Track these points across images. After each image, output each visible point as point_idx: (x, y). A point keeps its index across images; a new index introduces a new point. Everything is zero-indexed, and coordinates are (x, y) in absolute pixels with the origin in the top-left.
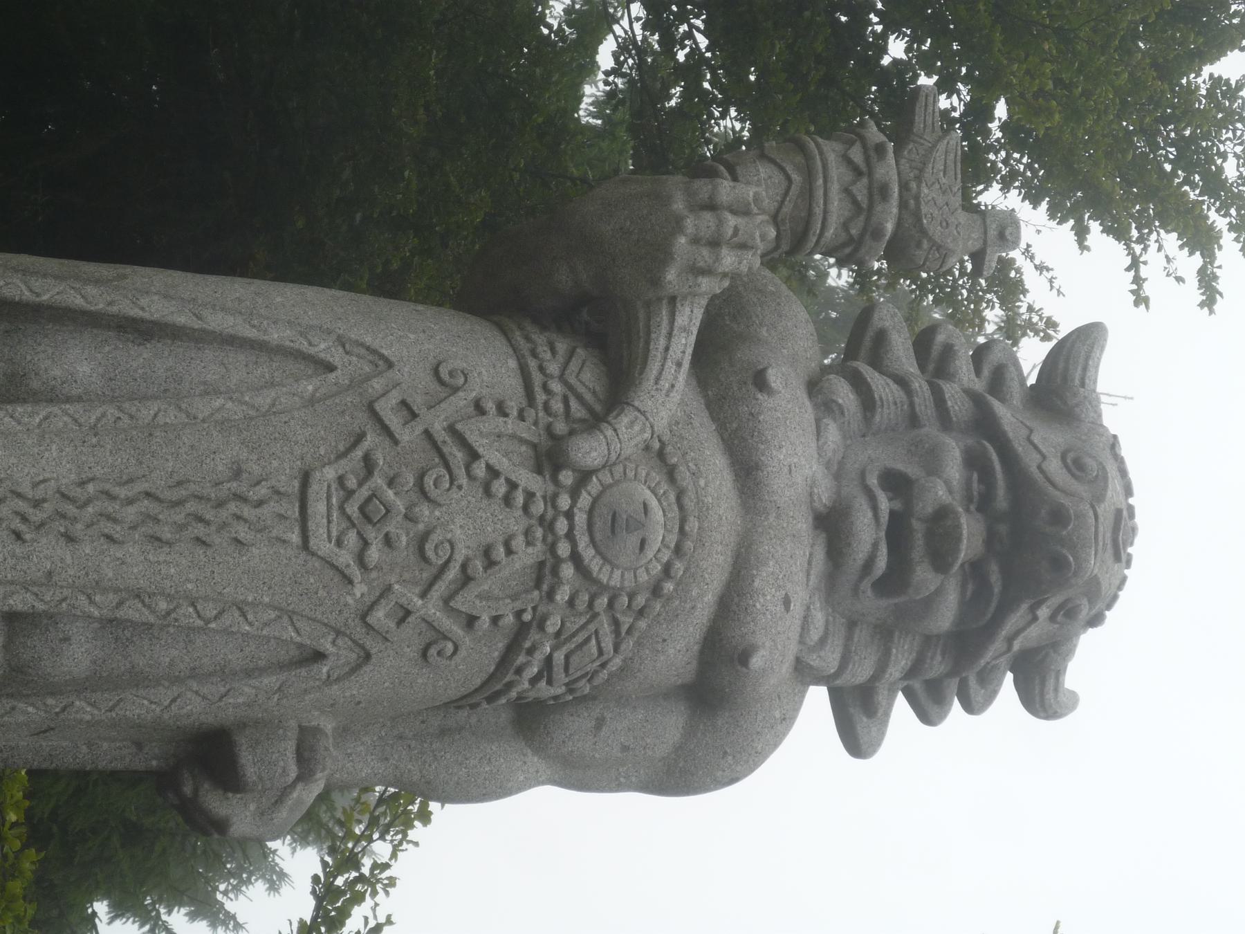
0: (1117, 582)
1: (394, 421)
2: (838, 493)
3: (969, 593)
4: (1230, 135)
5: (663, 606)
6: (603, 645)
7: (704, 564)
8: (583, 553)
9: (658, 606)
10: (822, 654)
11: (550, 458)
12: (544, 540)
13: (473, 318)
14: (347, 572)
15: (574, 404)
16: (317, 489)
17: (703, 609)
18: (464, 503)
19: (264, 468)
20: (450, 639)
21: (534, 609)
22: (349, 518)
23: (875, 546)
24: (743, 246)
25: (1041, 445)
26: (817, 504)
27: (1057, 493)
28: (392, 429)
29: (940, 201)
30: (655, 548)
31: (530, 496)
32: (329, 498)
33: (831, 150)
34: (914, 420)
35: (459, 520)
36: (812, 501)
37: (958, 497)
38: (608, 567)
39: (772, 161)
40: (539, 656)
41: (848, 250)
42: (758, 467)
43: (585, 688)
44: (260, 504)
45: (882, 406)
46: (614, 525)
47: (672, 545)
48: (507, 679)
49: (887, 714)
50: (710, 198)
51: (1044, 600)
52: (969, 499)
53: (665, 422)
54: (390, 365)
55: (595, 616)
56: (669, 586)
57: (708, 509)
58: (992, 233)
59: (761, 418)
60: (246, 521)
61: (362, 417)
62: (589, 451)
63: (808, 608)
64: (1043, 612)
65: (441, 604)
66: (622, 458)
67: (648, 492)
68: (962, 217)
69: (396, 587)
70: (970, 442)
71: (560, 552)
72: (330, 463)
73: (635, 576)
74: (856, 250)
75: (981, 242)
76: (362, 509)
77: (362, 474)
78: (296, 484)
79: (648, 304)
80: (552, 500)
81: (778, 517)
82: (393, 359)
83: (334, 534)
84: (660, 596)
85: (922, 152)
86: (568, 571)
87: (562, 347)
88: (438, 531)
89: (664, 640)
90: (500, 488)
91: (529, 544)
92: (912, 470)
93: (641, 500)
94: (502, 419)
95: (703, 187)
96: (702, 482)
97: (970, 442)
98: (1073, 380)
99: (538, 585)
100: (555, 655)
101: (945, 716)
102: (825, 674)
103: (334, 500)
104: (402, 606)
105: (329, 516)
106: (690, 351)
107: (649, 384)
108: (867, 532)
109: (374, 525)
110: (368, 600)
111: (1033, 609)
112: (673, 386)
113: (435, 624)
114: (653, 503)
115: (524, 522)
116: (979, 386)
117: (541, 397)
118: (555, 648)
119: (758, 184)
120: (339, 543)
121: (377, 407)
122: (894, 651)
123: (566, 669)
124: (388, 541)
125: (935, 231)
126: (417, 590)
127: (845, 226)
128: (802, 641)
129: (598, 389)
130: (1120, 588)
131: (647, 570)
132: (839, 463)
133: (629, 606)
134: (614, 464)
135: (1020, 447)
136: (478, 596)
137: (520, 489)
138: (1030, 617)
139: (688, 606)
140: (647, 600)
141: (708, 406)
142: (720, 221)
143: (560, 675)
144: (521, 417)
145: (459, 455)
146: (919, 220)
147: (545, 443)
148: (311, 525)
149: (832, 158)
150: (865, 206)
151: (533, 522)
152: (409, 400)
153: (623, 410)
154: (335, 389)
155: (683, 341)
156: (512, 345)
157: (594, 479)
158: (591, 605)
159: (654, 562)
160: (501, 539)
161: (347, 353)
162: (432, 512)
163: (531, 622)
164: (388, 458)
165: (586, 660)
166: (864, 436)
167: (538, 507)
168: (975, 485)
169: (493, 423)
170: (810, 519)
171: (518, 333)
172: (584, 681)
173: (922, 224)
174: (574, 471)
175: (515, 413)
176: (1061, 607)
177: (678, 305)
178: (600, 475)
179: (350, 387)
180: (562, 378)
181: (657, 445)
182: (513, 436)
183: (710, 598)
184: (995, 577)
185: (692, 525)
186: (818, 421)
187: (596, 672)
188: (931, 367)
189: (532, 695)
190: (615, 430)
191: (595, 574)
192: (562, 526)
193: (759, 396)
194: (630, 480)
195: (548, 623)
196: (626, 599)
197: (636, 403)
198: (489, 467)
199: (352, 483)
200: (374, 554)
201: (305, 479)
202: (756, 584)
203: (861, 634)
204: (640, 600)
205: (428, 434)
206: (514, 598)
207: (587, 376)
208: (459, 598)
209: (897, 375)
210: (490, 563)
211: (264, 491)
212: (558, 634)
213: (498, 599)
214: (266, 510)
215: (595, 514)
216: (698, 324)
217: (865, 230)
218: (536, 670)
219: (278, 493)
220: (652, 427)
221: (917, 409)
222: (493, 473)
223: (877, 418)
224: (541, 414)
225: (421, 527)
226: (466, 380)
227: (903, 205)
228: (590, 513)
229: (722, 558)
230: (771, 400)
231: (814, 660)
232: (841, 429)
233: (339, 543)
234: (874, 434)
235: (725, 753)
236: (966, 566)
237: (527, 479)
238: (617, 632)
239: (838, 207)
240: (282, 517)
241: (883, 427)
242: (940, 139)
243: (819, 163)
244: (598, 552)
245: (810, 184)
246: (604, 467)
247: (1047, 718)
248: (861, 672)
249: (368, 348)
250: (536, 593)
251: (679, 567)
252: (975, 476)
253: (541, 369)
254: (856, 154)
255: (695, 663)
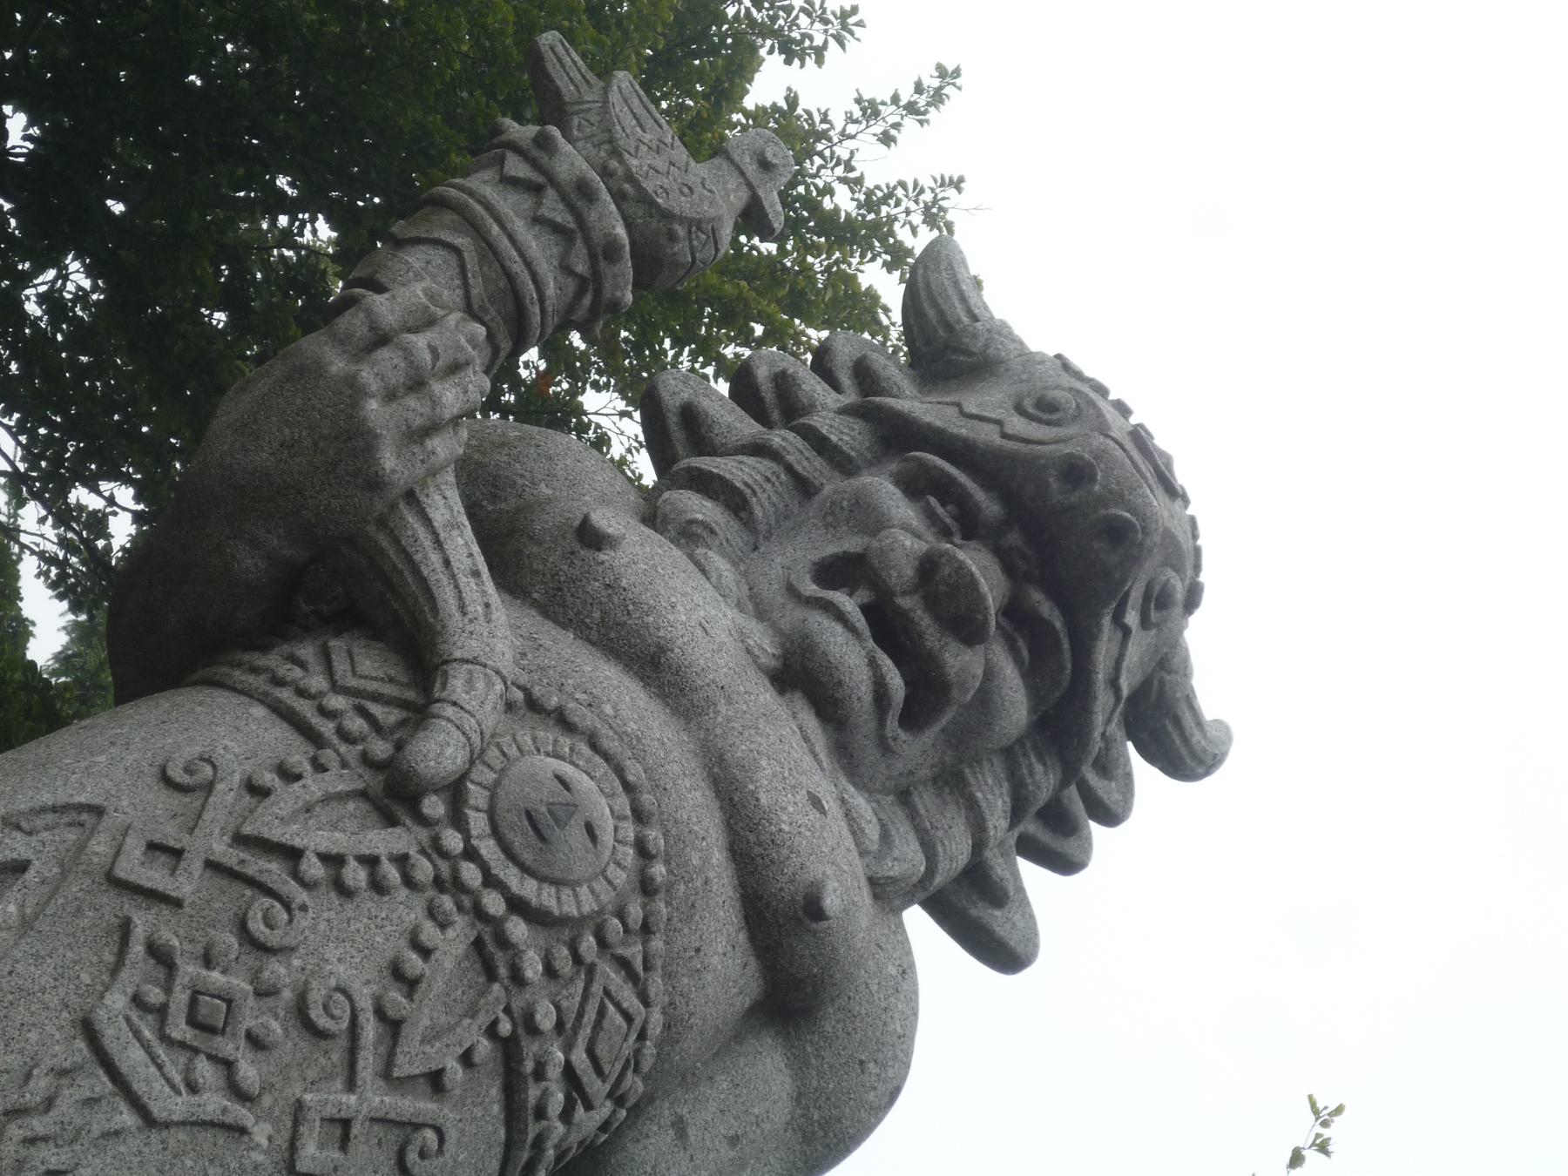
0: (1188, 528)
1: (155, 877)
2: (778, 631)
3: (1025, 653)
4: (818, 161)
5: (668, 904)
6: (625, 1005)
7: (683, 815)
8: (523, 893)
9: (660, 905)
10: (896, 853)
11: (395, 794)
12: (460, 909)
13: (167, 694)
14: (229, 1119)
15: (376, 709)
16: (114, 1034)
17: (719, 877)
18: (322, 926)
19: (21, 1052)
20: (424, 1125)
21: (508, 1010)
22: (183, 1045)
23: (872, 663)
24: (455, 368)
25: (981, 413)
26: (763, 660)
27: (1052, 447)
28: (161, 889)
29: (660, 163)
30: (610, 828)
31: (402, 860)
32: (137, 1034)
33: (483, 183)
34: (804, 488)
35: (332, 953)
36: (755, 659)
37: (931, 538)
38: (567, 891)
39: (418, 241)
40: (554, 1072)
41: (587, 300)
42: (662, 649)
43: (635, 1085)
44: (49, 1103)
45: (754, 492)
46: (539, 828)
47: (629, 812)
48: (531, 1136)
49: (1020, 889)
50: (372, 329)
51: (1127, 594)
52: (946, 533)
53: (509, 656)
54: (98, 811)
55: (591, 970)
56: (659, 870)
57: (639, 740)
58: (751, 169)
59: (624, 583)
60: (45, 1139)
61: (112, 905)
62: (439, 751)
63: (843, 801)
64: (1132, 618)
65: (382, 1084)
66: (487, 736)
67: (549, 760)
68: (700, 170)
69: (308, 1097)
70: (894, 467)
71: (492, 911)
72: (107, 988)
73: (610, 882)
74: (598, 293)
75: (745, 189)
76: (192, 1021)
77: (161, 974)
78: (81, 1044)
79: (382, 522)
80: (436, 848)
81: (729, 702)
82: (97, 801)
83: (178, 1079)
84: (656, 892)
85: (594, 118)
86: (518, 929)
87: (307, 651)
88: (314, 984)
89: (698, 950)
90: (356, 875)
91: (443, 926)
92: (852, 544)
93: (550, 775)
94: (296, 786)
95: (352, 322)
96: (608, 710)
97: (894, 467)
98: (959, 321)
99: (491, 974)
100: (573, 1058)
101: (1090, 845)
102: (915, 879)
103: (147, 1034)
104: (332, 1120)
105: (154, 1059)
106: (476, 549)
107: (455, 621)
108: (851, 655)
109: (223, 1032)
110: (282, 1141)
111: (1118, 619)
112: (487, 605)
113: (392, 1116)
114: (568, 770)
115: (418, 903)
116: (850, 397)
117: (327, 728)
118: (568, 1048)
119: (418, 277)
120: (193, 1088)
121: (120, 873)
122: (979, 795)
123: (599, 1071)
124: (256, 1042)
125: (681, 205)
126: (339, 1084)
127: (565, 268)
128: (863, 853)
129: (393, 672)
130: (1195, 537)
131: (618, 864)
132: (750, 598)
133: (627, 930)
134: (483, 751)
135: (962, 429)
136: (425, 1040)
137: (384, 859)
138: (1119, 634)
139: (698, 883)
140: (644, 906)
141: (545, 613)
142: (405, 349)
143: (597, 1088)
144: (319, 767)
145: (274, 866)
146: (653, 203)
147: (375, 782)
148: (138, 1087)
149: (490, 192)
150: (572, 225)
151: (430, 893)
152: (157, 838)
153: (446, 673)
154: (46, 889)
155: (461, 541)
156: (241, 692)
157: (469, 785)
158: (577, 959)
159: (620, 848)
160: (403, 943)
161: (30, 834)
162: (289, 966)
163: (514, 1031)
164: (181, 932)
165: (616, 1044)
166: (756, 548)
167: (424, 870)
168: (940, 510)
169: (287, 798)
170: (767, 682)
171: (237, 673)
172: (630, 1073)
173: (658, 206)
174: (436, 792)
175: (307, 767)
176: (1147, 597)
177: (422, 498)
178: (474, 776)
179: (64, 873)
180: (336, 688)
181: (519, 695)
182: (327, 799)
183: (718, 857)
184: (1046, 608)
185: (634, 772)
186: (691, 556)
187: (637, 1052)
188: (775, 415)
189: (574, 1139)
190: (455, 704)
191: (556, 912)
192: (471, 874)
193: (602, 557)
194: (517, 759)
195: (538, 1017)
196: (616, 921)
197: (458, 654)
198: (325, 858)
199: (155, 995)
200: (249, 1072)
201: (88, 1030)
202: (763, 801)
203: (925, 800)
204: (635, 912)
205: (212, 866)
206: (472, 1012)
207: (367, 665)
208: (400, 1059)
209: (743, 446)
210: (410, 985)
211: (43, 1083)
212: (560, 1026)
213: (451, 1028)
214: (64, 1107)
215: (504, 830)
216: (462, 510)
217: (592, 257)
218: (561, 1096)
219: (64, 1073)
220: (498, 672)
221: (799, 469)
222: (334, 861)
223: (758, 512)
224: (343, 748)
225: (287, 994)
226: (214, 766)
227: (619, 197)
228: (496, 832)
229: (698, 794)
230: (620, 554)
231: (891, 869)
232: (723, 554)
233: (193, 1088)
234: (767, 538)
235: (862, 1062)
236: (1001, 619)
237: (384, 841)
238: (632, 977)
239: (540, 248)
240: (91, 1102)
241: (773, 520)
242: (606, 91)
243: (477, 207)
244: (542, 879)
245: (486, 241)
246: (472, 762)
247: (1207, 773)
248: (956, 850)
249: (54, 809)
250: (496, 987)
251: (653, 834)
252: (932, 500)
253: (302, 693)
254: (516, 167)
255: (752, 960)
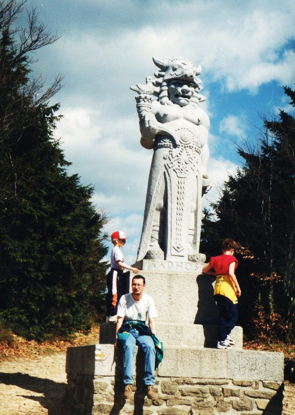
23: (185, 100)
